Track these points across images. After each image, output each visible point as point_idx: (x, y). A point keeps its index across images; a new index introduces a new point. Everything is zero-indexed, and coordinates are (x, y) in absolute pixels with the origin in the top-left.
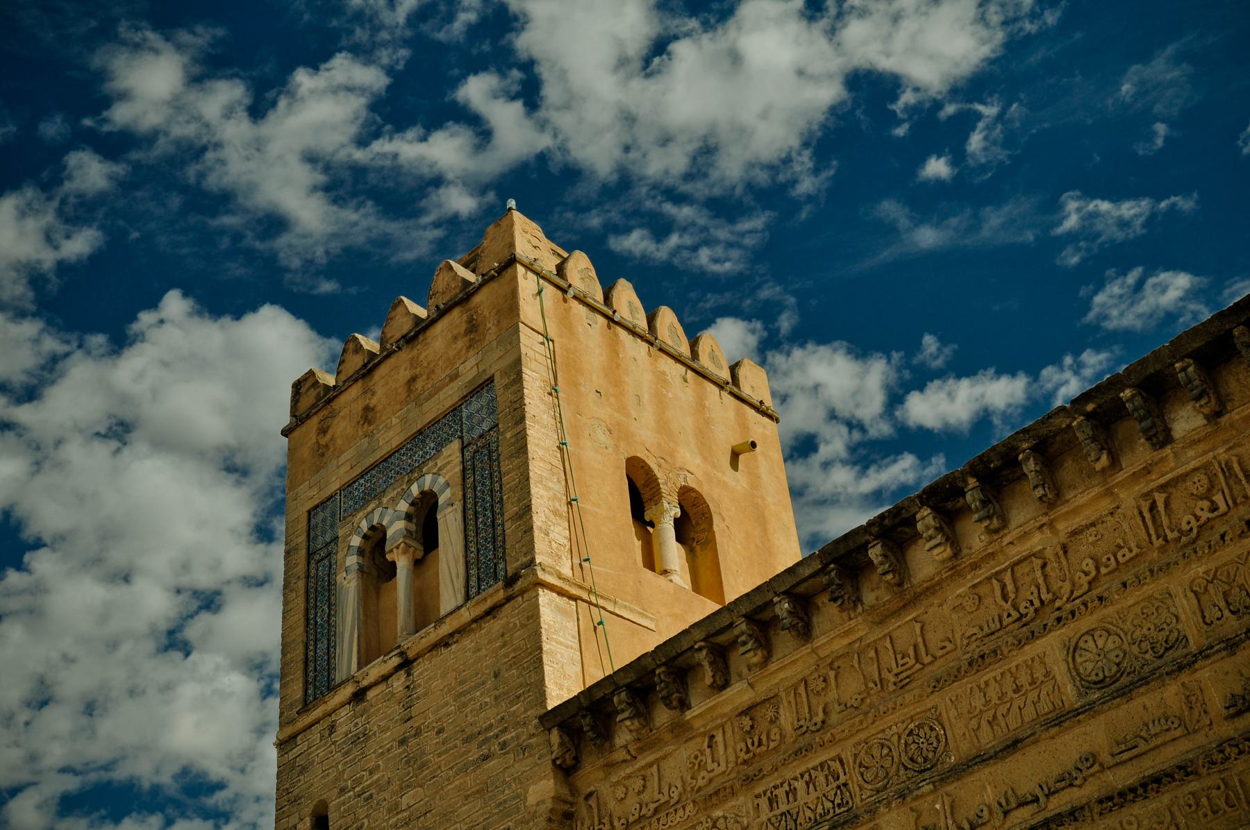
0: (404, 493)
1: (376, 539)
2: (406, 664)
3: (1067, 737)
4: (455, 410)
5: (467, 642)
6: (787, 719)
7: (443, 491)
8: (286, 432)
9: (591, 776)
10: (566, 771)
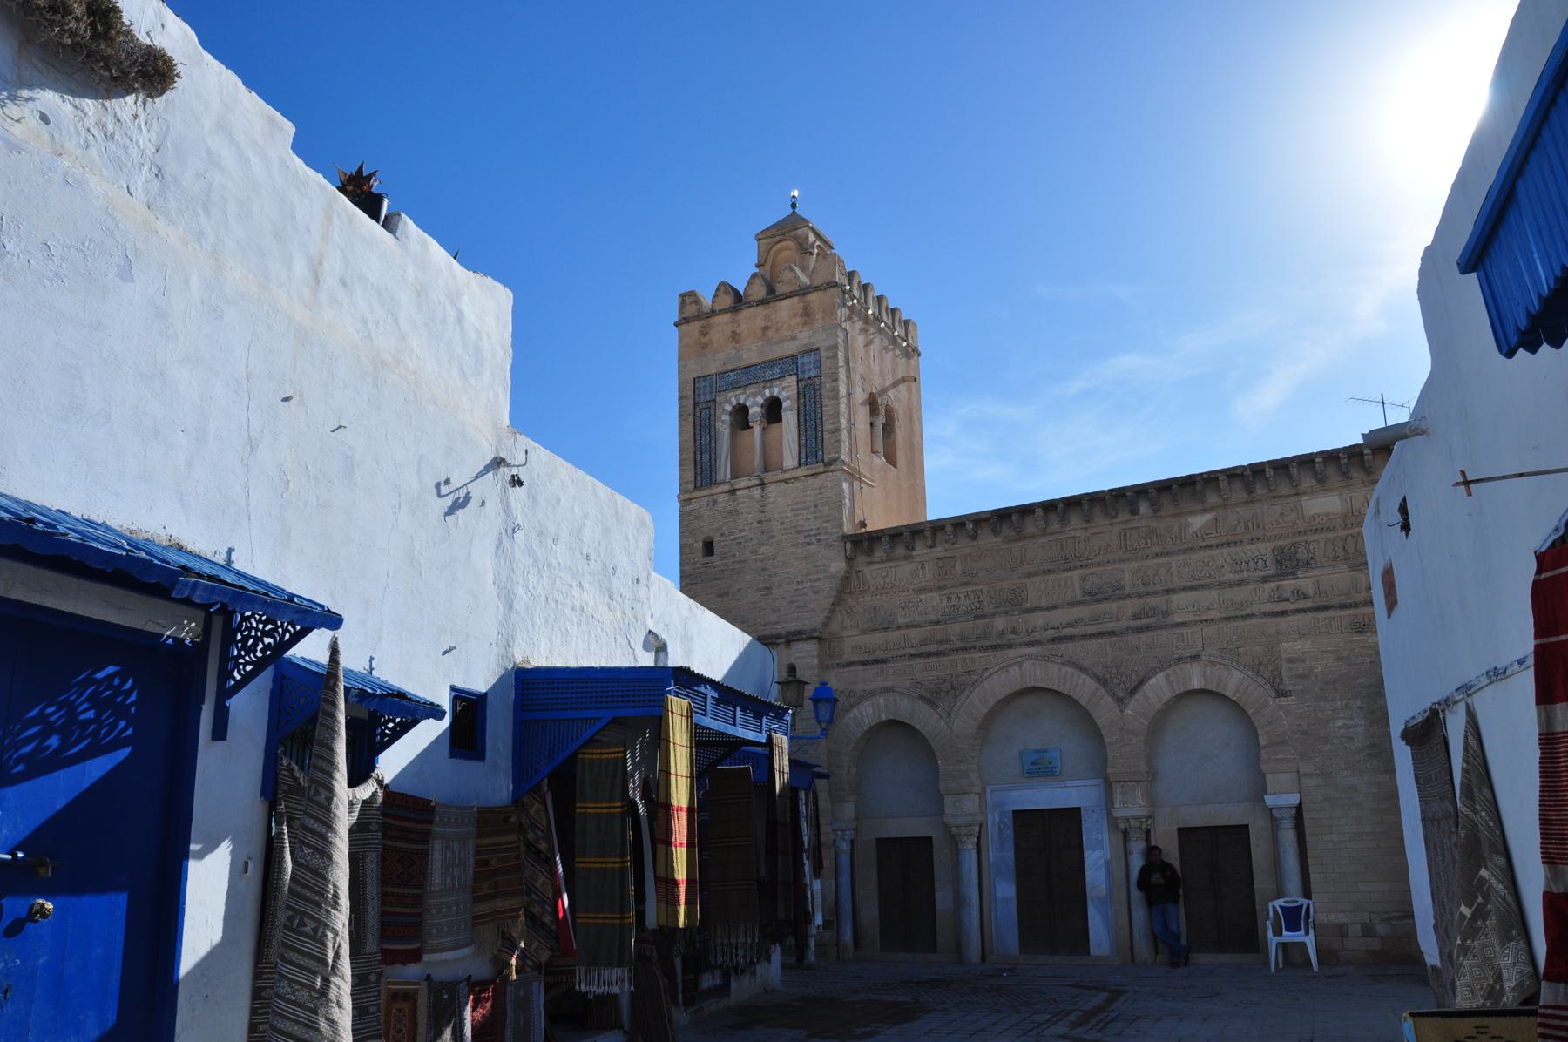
0: (761, 393)
1: (741, 412)
2: (763, 484)
4: (794, 357)
5: (798, 484)
6: (959, 568)
8: (676, 325)
10: (849, 560)
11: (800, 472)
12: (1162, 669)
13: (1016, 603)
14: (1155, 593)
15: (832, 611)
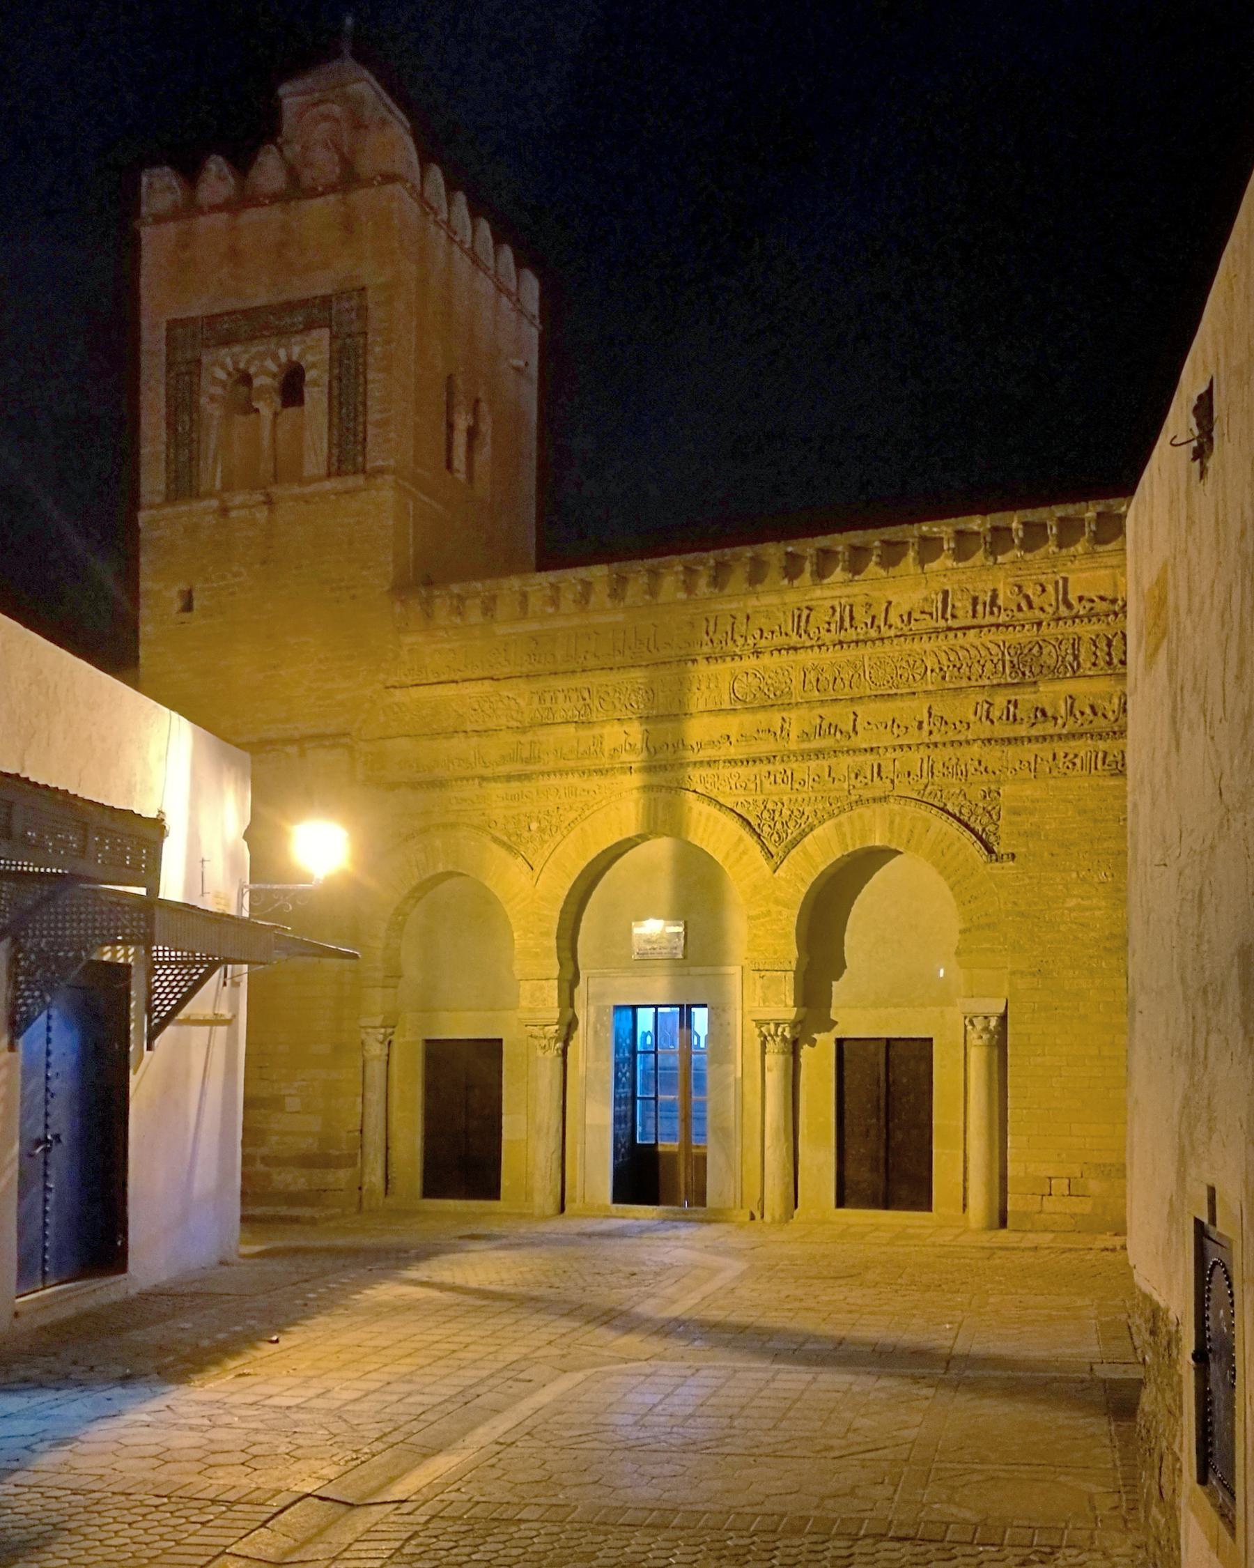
4: (326, 300)
11: (328, 485)
12: (832, 815)
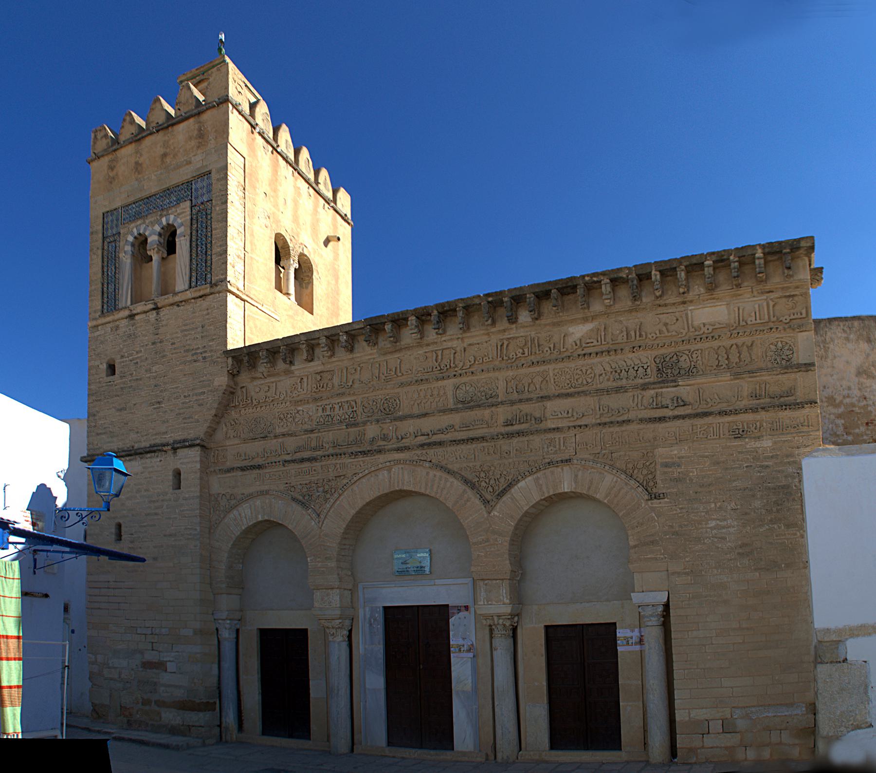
3: (446, 417)
7: (179, 227)
9: (244, 378)
13: (389, 412)
14: (529, 400)
15: (218, 423)
